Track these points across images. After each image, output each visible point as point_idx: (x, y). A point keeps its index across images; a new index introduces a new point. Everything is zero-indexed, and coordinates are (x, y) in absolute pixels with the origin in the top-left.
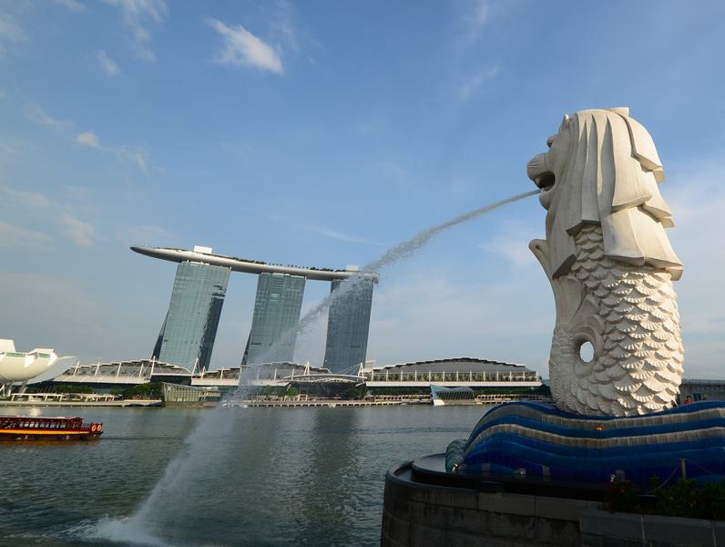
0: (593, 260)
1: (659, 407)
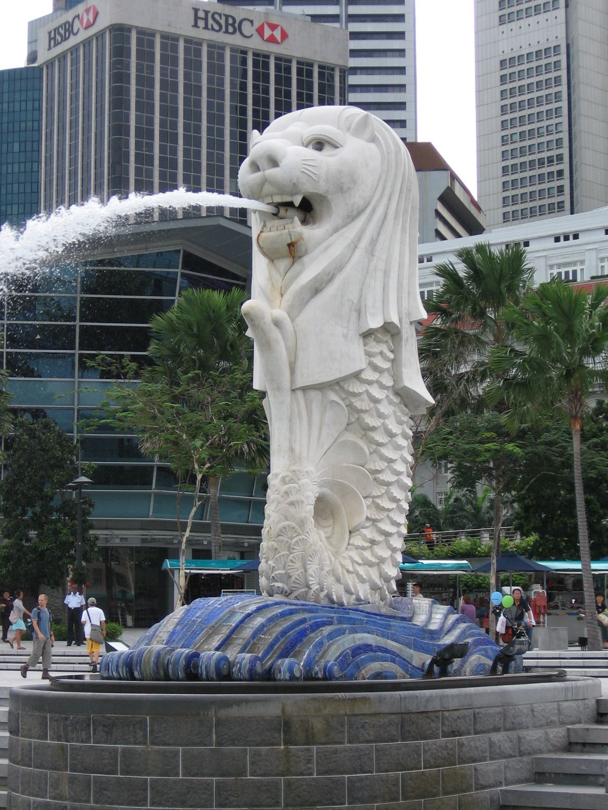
0: (382, 387)
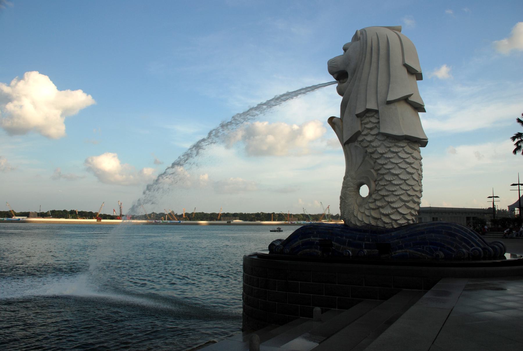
1: (403, 222)
